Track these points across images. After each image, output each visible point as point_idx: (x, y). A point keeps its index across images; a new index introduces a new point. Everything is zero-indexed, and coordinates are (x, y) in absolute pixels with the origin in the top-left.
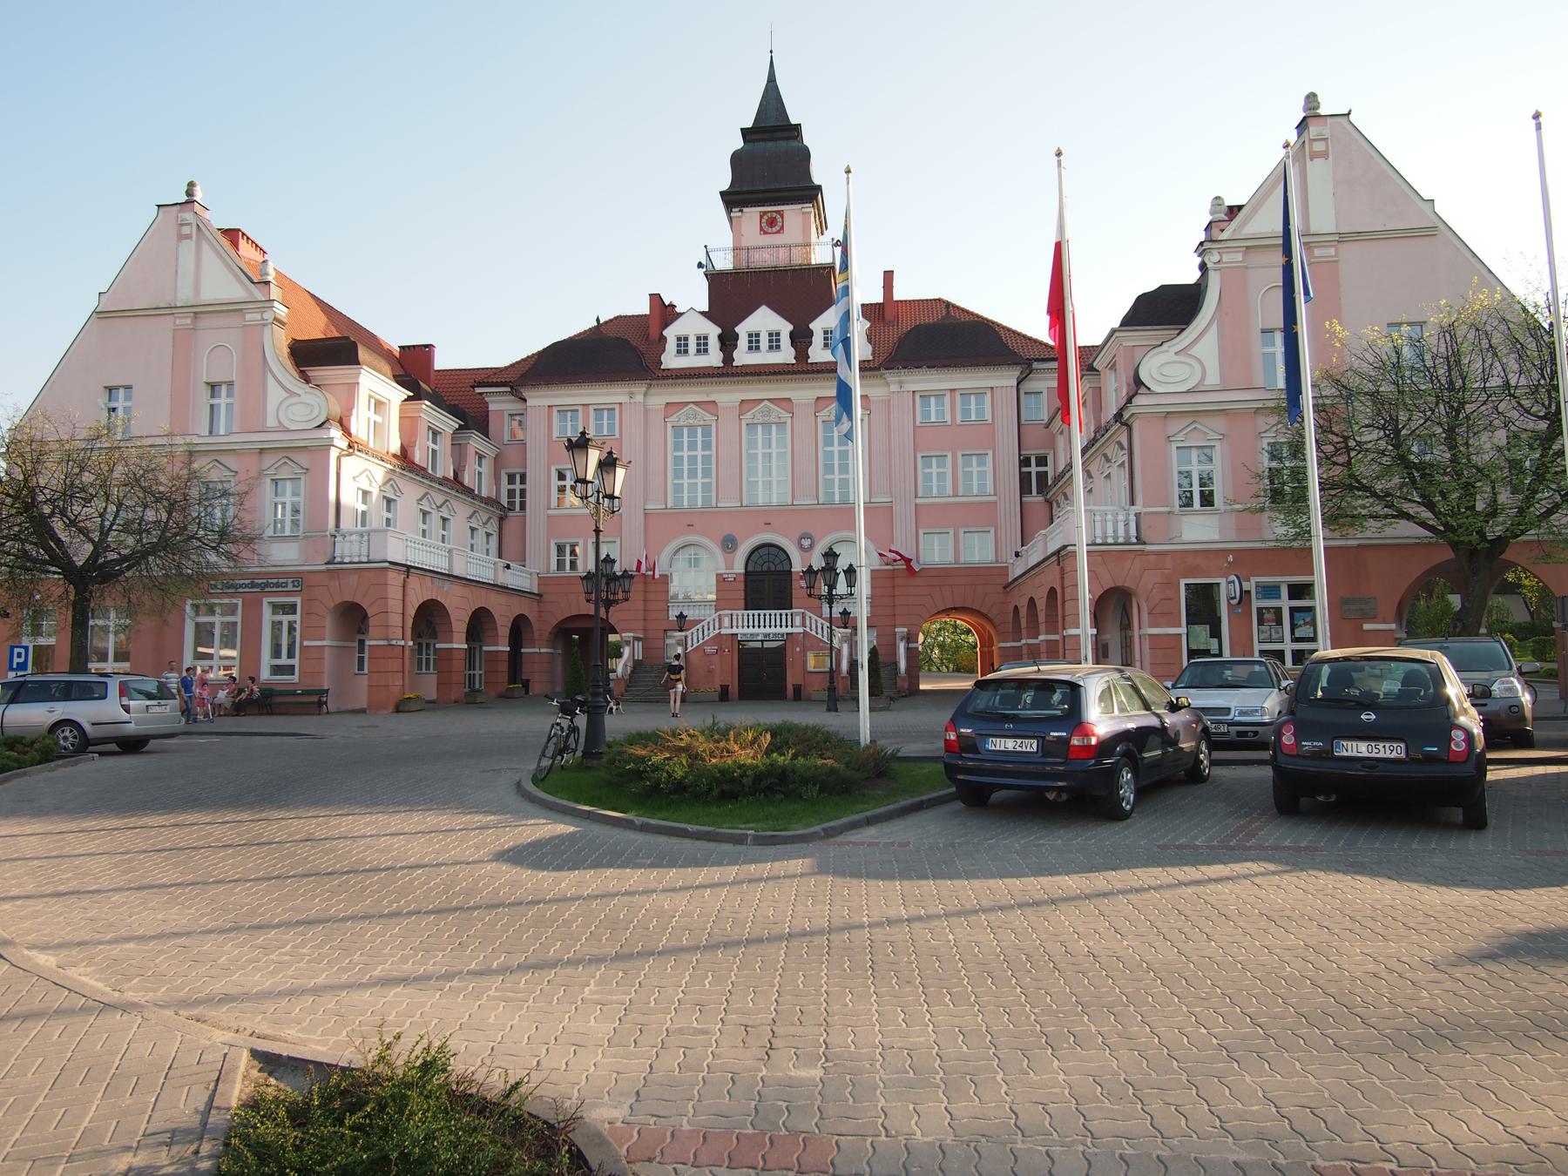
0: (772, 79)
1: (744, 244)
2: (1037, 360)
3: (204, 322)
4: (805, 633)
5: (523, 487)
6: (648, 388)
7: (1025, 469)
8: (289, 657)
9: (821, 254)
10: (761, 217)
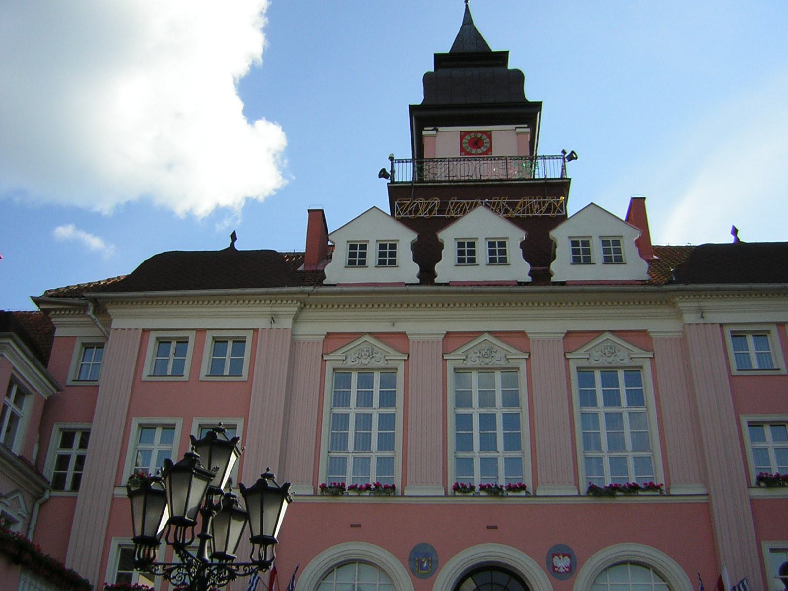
5: (82, 452)
6: (301, 309)
9: (549, 170)
10: (462, 138)
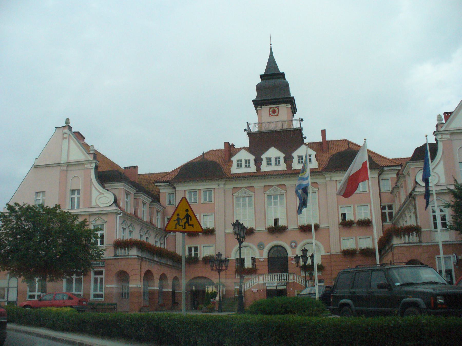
1: (263, 121)
2: (386, 166)
3: (70, 168)
4: (294, 282)
6: (225, 182)
7: (383, 211)
8: (100, 291)
9: (296, 125)
10: (270, 110)
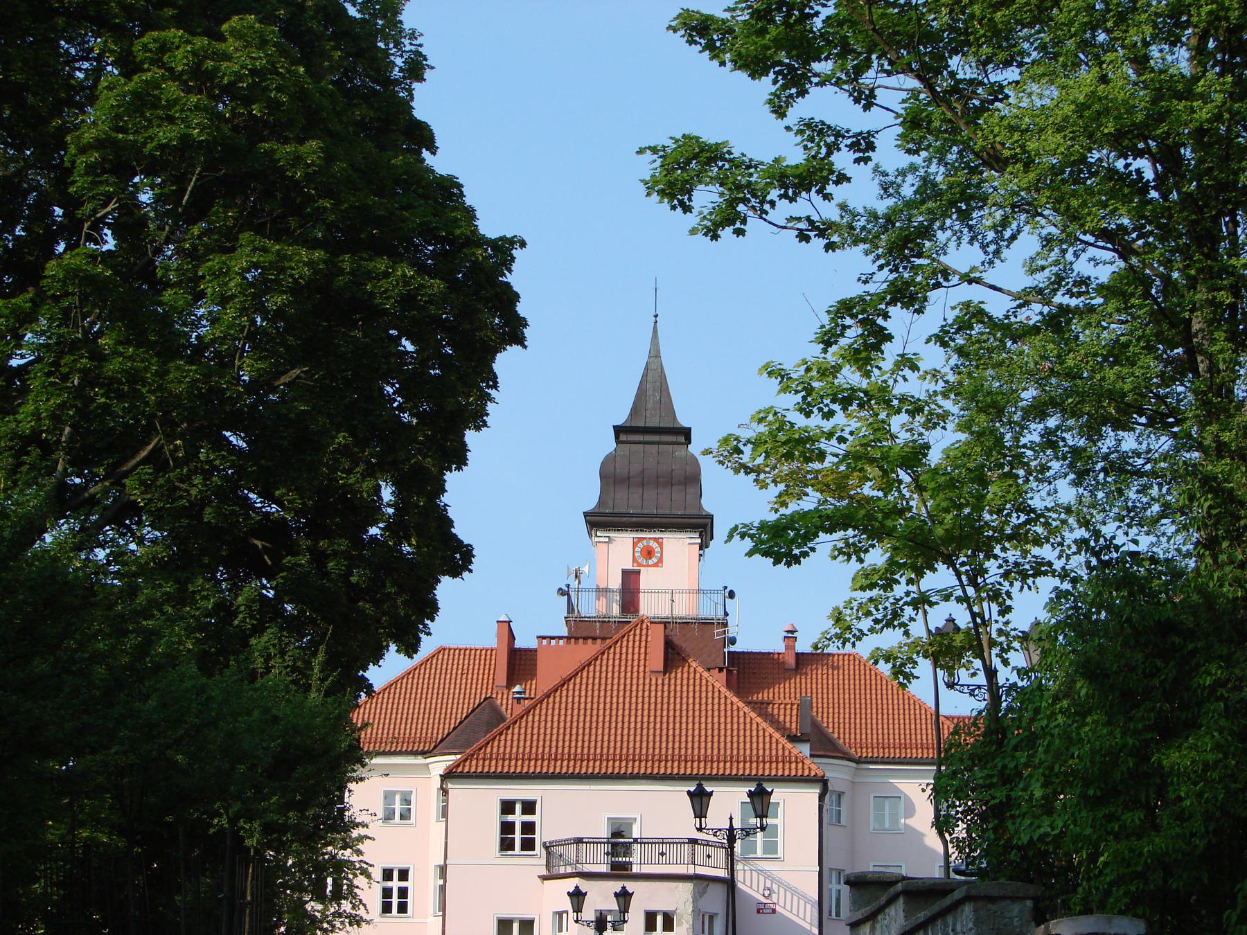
0: (655, 353)
10: (635, 545)
